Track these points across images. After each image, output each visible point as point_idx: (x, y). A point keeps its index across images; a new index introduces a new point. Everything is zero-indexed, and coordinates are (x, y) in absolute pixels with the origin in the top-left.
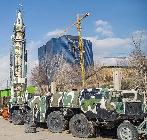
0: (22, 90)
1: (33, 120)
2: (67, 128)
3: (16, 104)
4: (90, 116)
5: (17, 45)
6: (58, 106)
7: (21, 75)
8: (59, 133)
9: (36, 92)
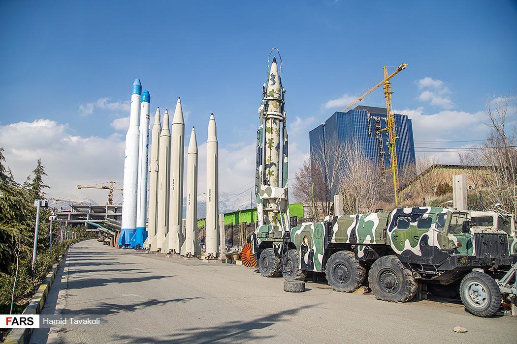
0: (278, 210)
1: (300, 268)
2: (365, 283)
3: (267, 237)
4: (409, 261)
5: (269, 125)
6: (348, 242)
7: (278, 182)
8: (350, 292)
9: (306, 215)
